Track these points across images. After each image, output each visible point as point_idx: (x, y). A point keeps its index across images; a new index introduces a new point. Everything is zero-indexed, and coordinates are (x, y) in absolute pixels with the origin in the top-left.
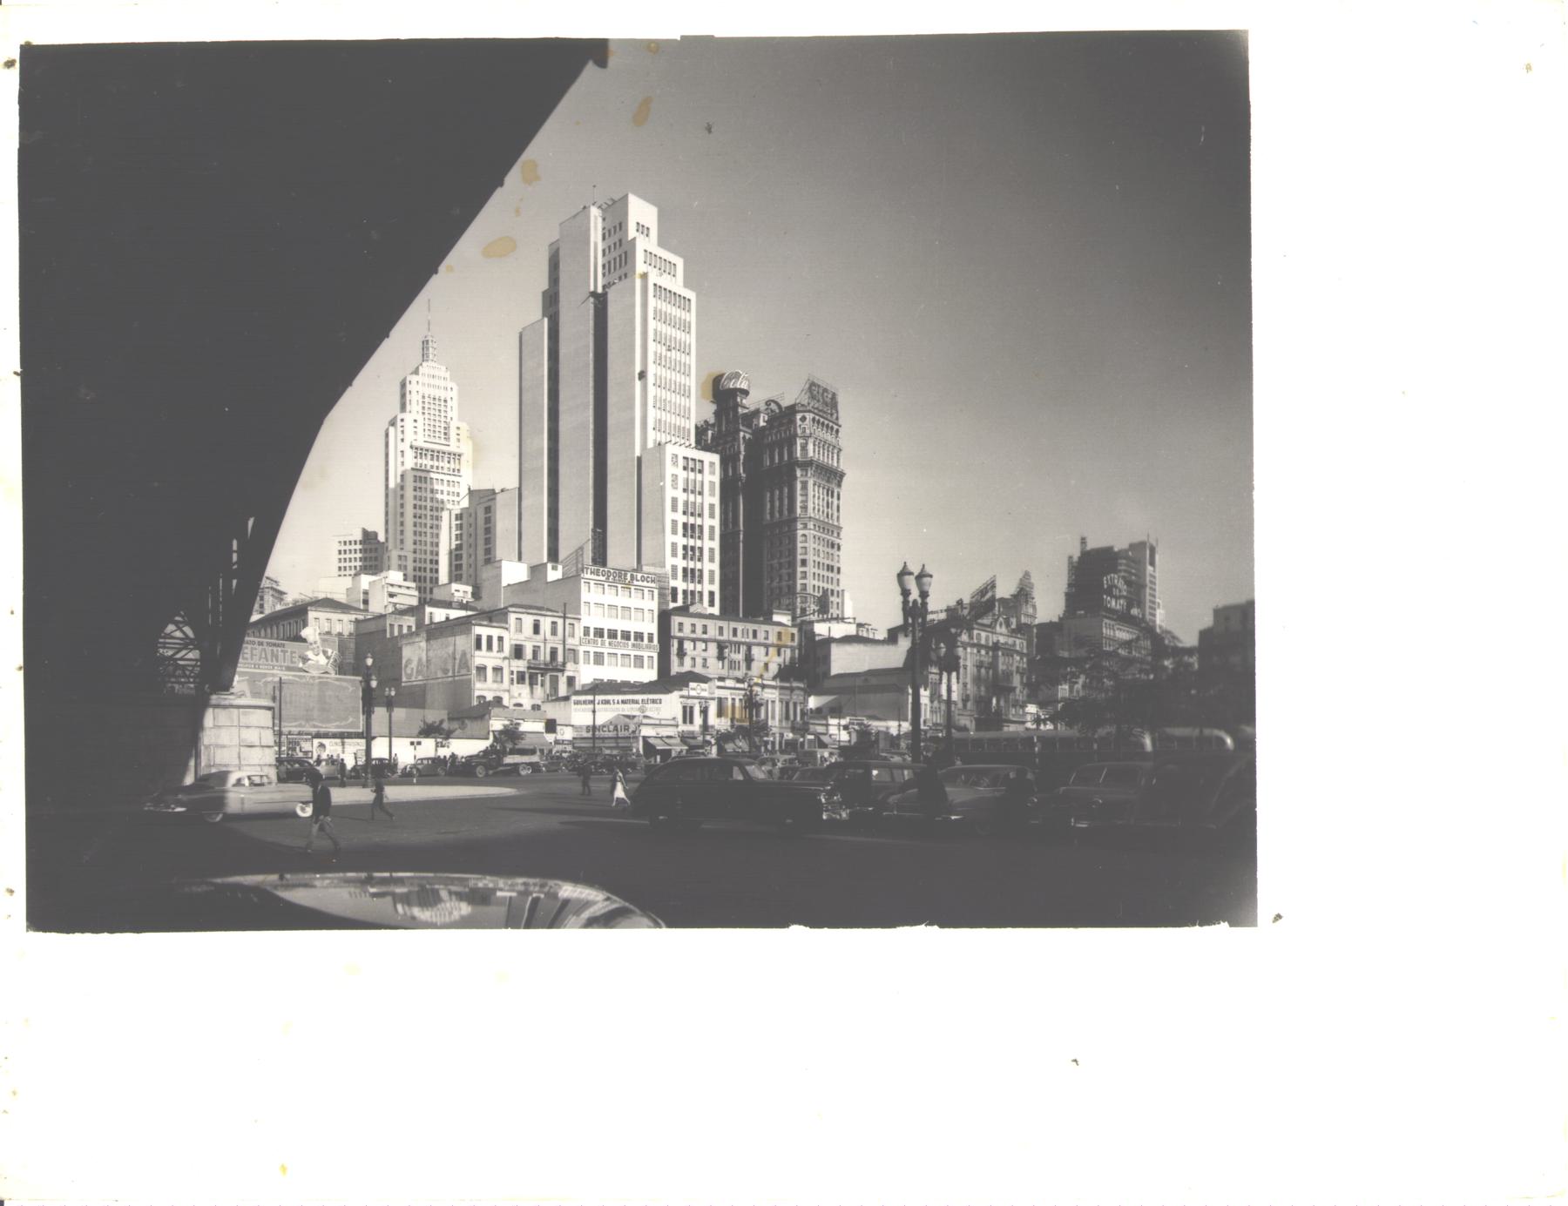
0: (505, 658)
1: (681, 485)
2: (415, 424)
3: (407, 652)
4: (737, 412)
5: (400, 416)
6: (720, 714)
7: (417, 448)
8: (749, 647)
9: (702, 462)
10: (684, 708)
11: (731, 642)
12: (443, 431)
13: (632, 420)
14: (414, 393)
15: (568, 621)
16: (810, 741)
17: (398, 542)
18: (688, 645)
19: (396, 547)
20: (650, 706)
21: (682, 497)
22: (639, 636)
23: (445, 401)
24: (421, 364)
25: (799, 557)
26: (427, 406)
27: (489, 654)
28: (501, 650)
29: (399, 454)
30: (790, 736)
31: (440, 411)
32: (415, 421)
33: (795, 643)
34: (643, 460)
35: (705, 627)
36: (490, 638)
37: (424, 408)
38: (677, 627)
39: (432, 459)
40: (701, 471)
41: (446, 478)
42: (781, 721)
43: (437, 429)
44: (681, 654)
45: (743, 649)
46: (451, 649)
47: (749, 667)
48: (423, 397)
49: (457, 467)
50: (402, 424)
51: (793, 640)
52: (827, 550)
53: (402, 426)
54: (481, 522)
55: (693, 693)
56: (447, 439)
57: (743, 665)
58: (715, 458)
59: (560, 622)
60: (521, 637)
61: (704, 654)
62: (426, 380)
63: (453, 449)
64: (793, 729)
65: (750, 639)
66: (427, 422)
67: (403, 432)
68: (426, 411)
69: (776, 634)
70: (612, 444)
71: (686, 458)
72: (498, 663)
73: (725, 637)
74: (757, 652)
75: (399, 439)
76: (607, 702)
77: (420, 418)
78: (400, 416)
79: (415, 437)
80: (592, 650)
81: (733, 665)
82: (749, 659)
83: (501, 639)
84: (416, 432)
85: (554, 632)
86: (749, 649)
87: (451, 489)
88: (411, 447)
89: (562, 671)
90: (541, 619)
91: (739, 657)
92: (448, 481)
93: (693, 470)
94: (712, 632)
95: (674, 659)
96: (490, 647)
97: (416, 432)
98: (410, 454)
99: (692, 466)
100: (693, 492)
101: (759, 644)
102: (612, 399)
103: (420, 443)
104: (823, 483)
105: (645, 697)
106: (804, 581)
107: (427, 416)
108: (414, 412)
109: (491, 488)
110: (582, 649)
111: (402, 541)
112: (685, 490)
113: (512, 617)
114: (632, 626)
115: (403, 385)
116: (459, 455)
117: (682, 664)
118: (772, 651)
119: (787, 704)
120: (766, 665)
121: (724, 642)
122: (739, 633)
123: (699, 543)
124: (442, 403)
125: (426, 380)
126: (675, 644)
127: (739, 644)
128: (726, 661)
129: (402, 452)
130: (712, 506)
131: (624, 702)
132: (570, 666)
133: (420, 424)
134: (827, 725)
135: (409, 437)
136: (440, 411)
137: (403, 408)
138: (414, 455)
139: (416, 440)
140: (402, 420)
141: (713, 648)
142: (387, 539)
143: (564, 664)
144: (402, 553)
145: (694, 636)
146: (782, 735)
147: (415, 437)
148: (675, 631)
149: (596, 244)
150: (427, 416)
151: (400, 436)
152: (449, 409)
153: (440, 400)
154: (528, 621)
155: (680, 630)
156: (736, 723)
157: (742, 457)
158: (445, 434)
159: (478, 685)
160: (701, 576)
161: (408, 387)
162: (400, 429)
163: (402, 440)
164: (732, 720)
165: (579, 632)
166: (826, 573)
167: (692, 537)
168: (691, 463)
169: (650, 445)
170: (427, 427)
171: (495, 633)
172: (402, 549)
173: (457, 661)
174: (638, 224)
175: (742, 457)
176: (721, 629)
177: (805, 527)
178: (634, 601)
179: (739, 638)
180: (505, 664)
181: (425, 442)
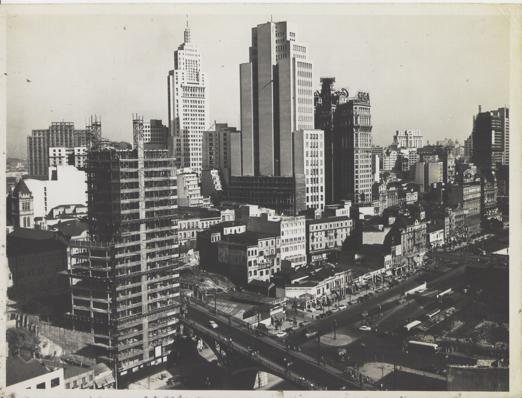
0: (257, 257)
1: (310, 145)
2: (183, 75)
3: (220, 250)
4: (330, 93)
5: (175, 71)
6: (327, 288)
7: (184, 87)
8: (336, 230)
9: (317, 135)
10: (318, 290)
11: (329, 230)
12: (196, 76)
13: (290, 116)
14: (182, 59)
15: (277, 239)
16: (353, 286)
17: (176, 132)
18: (315, 234)
19: (174, 135)
20: (308, 290)
21: (309, 150)
22: (300, 238)
23: (197, 62)
24: (184, 44)
25: (355, 164)
26: (188, 65)
27: (253, 257)
28: (256, 254)
29: (175, 90)
30: (347, 287)
31: (194, 72)
32: (183, 73)
33: (352, 226)
34: (295, 134)
35: (321, 226)
36: (252, 251)
37: (186, 66)
38: (311, 228)
39: (191, 91)
40: (317, 138)
41: (197, 100)
42: (345, 283)
43: (193, 76)
44: (313, 237)
45: (334, 231)
46: (239, 254)
47: (336, 238)
48: (186, 61)
49: (203, 94)
50: (177, 75)
51: (351, 224)
52: (365, 159)
53: (177, 76)
54: (222, 139)
55: (320, 285)
56: (198, 80)
57: (334, 237)
58: (322, 132)
59: (274, 240)
60: (262, 248)
61: (321, 236)
62: (187, 52)
63: (200, 86)
64: (348, 285)
65: (336, 227)
66: (188, 72)
67: (177, 79)
68: (188, 67)
69: (345, 224)
70: (282, 125)
71: (311, 135)
72: (255, 259)
73: (328, 229)
74: (339, 231)
75: (175, 83)
76: (296, 289)
77: (185, 72)
78: (175, 71)
79: (183, 81)
80: (284, 247)
81: (330, 238)
82: (336, 235)
83: (256, 251)
84: (183, 79)
85: (272, 244)
86: (336, 231)
87: (200, 109)
88: (181, 86)
89: (275, 257)
90: (268, 241)
91: (332, 234)
92: (199, 101)
93: (314, 138)
94: (323, 228)
95: (311, 240)
96: (252, 254)
97: (183, 79)
98: (181, 90)
99: (314, 137)
100: (314, 156)
101: (339, 228)
102: (282, 106)
103: (185, 85)
104: (365, 132)
105: (307, 288)
106: (357, 179)
107: (188, 70)
108: (182, 68)
109: (225, 123)
110: (281, 248)
111: (178, 132)
112: (311, 147)
113: (259, 242)
114: (297, 236)
115: (176, 54)
116: (204, 88)
117: (313, 241)
118: (344, 230)
119: (346, 277)
120: (342, 235)
121: (328, 230)
122: (332, 226)
123: (317, 185)
124: (195, 63)
125: (187, 52)
126: (311, 234)
127: (332, 230)
128: (328, 237)
129: (177, 89)
130: (321, 152)
131: (301, 289)
132: (278, 254)
133: (185, 75)
134: (358, 279)
135: (180, 81)
136: (194, 69)
137: (176, 68)
138: (183, 90)
139: (183, 83)
140: (177, 73)
141: (323, 233)
142: (170, 125)
143: (276, 254)
144: (178, 138)
145: (317, 230)
146: (345, 287)
147: (183, 81)
148: (311, 230)
149: (273, 38)
150: (188, 70)
151: (176, 81)
152: (198, 66)
153: (194, 61)
154: (264, 242)
155: (313, 229)
156: (332, 290)
157: (332, 118)
158: (197, 78)
159: (249, 268)
160: (318, 180)
161: (179, 56)
162: (175, 77)
163: (177, 83)
164: (331, 289)
165: (280, 242)
166: (365, 169)
167: (314, 183)
168: (313, 136)
169: (297, 129)
170: (188, 75)
171: (254, 249)
172: (178, 136)
173: (241, 259)
174: (290, 33)
175: (332, 118)
176: (326, 226)
177: (357, 152)
178: (298, 227)
179: (332, 228)
180: (257, 259)
181: (188, 83)
